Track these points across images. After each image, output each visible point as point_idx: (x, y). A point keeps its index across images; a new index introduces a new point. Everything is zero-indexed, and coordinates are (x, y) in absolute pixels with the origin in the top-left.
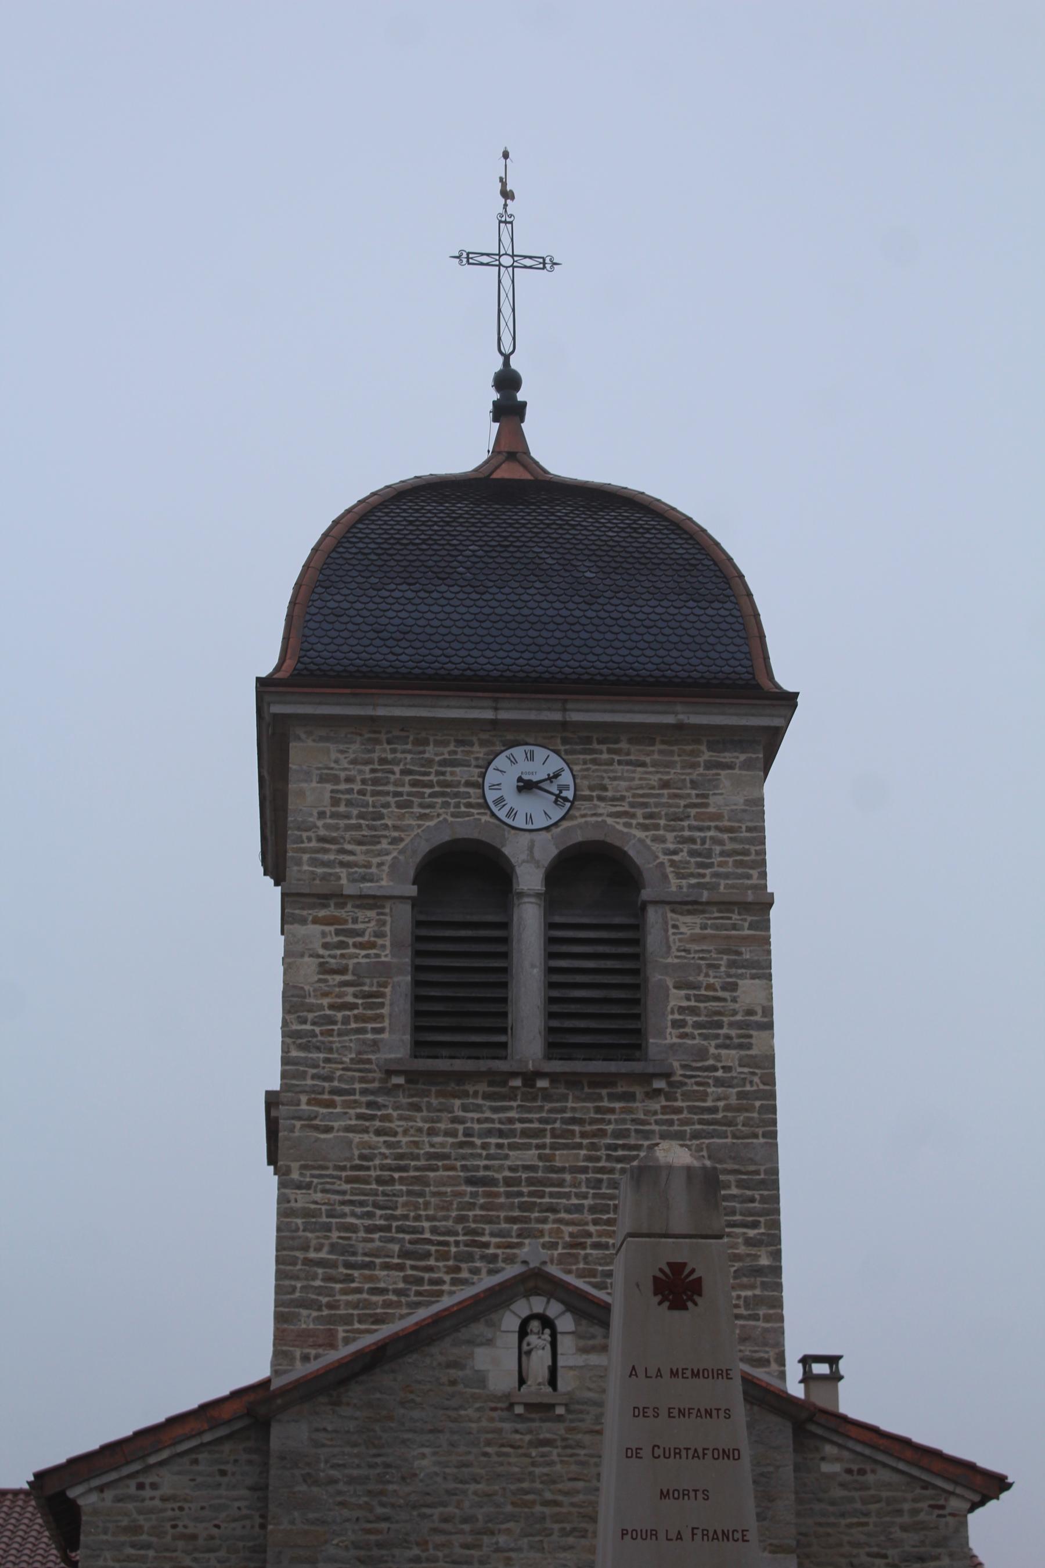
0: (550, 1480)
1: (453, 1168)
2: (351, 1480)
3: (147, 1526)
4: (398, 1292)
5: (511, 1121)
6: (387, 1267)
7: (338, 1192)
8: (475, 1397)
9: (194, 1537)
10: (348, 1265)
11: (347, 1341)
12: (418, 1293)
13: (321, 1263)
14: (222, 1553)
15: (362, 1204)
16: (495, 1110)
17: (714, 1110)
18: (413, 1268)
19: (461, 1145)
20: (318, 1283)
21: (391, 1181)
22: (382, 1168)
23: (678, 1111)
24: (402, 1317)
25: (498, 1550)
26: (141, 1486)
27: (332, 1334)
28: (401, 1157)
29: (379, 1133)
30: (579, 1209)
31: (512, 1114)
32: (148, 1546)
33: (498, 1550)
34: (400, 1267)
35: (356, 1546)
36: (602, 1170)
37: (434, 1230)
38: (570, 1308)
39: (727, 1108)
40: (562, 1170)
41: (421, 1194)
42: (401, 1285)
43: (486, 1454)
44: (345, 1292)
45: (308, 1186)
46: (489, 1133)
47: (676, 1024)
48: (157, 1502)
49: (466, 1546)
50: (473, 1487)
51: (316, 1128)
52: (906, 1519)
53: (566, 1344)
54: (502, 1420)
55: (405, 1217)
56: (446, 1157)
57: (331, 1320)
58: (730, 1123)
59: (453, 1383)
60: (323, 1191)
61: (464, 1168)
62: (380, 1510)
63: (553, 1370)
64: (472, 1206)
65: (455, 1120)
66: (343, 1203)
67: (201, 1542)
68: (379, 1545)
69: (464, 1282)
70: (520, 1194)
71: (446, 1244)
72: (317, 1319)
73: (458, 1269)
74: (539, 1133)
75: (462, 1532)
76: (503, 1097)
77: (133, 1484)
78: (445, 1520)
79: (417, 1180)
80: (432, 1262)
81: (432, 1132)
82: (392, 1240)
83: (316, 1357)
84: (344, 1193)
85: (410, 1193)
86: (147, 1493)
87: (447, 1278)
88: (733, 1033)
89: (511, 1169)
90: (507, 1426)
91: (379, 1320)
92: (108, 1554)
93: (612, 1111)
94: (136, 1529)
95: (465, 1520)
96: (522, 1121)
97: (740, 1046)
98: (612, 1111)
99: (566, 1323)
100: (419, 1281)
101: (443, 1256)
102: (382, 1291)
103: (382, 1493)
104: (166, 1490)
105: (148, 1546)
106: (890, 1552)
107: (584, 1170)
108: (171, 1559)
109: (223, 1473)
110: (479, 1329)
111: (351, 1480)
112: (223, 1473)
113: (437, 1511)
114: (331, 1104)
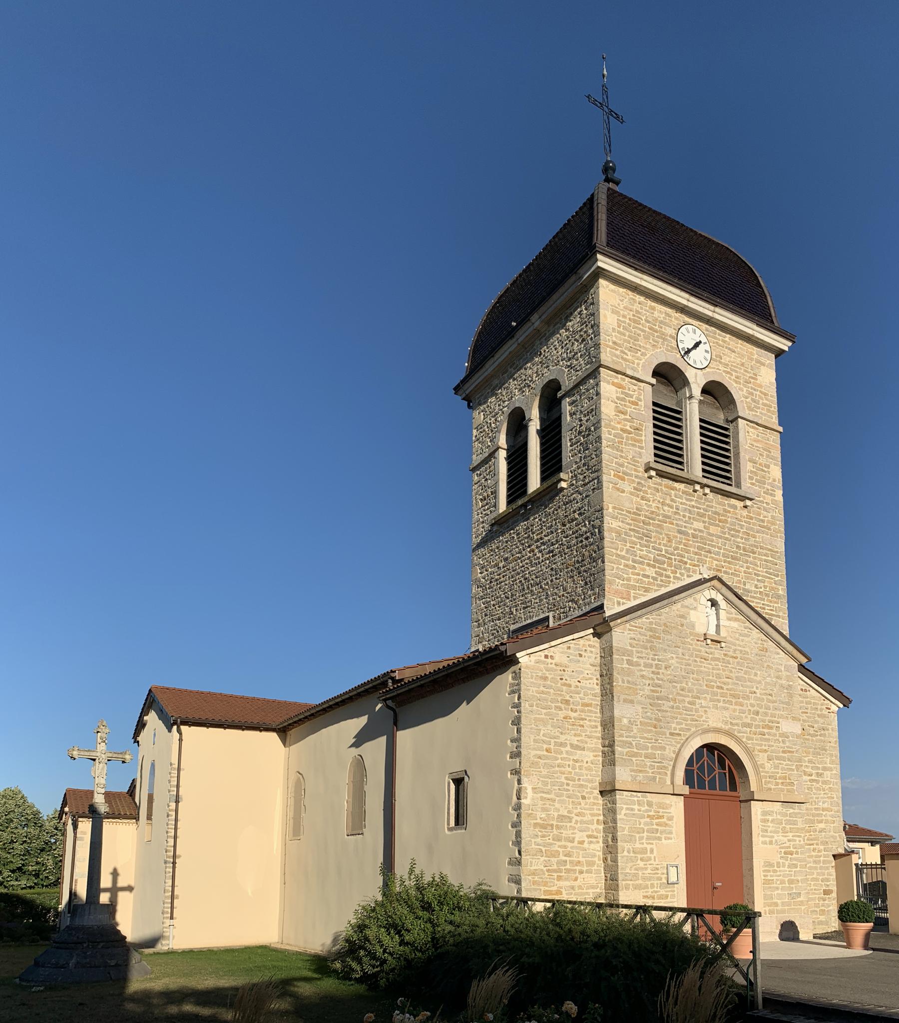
0: (718, 676)
1: (673, 524)
2: (646, 665)
3: (550, 677)
4: (655, 579)
5: (693, 506)
6: (649, 565)
7: (628, 524)
8: (691, 634)
9: (570, 686)
10: (634, 561)
11: (635, 598)
12: (662, 581)
13: (623, 557)
14: (581, 695)
15: (637, 532)
16: (687, 500)
17: (763, 521)
18: (659, 568)
19: (676, 513)
20: (622, 567)
21: (649, 524)
22: (646, 516)
23: (751, 518)
24: (656, 590)
25: (702, 707)
26: (546, 657)
27: (629, 594)
28: (652, 513)
29: (643, 498)
30: (718, 554)
31: (693, 503)
32: (551, 687)
33: (702, 707)
34: (654, 567)
35: (648, 697)
36: (726, 539)
37: (666, 552)
38: (726, 599)
39: (768, 522)
40: (712, 535)
41: (661, 534)
42: (654, 575)
43: (696, 661)
44: (633, 574)
45: (617, 518)
46: (686, 509)
47: (751, 478)
48: (553, 666)
49: (689, 703)
50: (691, 676)
51: (618, 489)
52: (819, 712)
53: (722, 614)
54: (701, 646)
55: (655, 542)
56: (669, 517)
57: (628, 587)
58: (769, 529)
59: (682, 625)
60: (622, 522)
61: (677, 525)
62: (656, 681)
63: (718, 626)
64: (680, 543)
65: (672, 500)
66: (630, 530)
67: (573, 688)
68: (658, 698)
69: (678, 578)
70: (697, 542)
71: (671, 559)
72: (622, 585)
73: (676, 572)
74: (703, 515)
75: (688, 696)
76: (690, 495)
77: (542, 654)
78: (682, 690)
79: (659, 526)
80: (665, 566)
81: (663, 504)
82: (650, 552)
83: (623, 604)
84: (630, 525)
85: (657, 532)
86: (549, 660)
87: (672, 575)
88: (769, 488)
89: (695, 530)
90: (703, 649)
91: (647, 590)
92: (535, 689)
93: (729, 512)
94: (545, 678)
95: (689, 692)
96: (698, 508)
97: (771, 495)
98: (729, 512)
99: (722, 604)
100: (661, 575)
101: (670, 565)
102: (648, 577)
103: (658, 673)
104: (557, 659)
105: (551, 687)
106: (816, 726)
107: (720, 537)
108: (561, 695)
109: (581, 655)
110: (689, 601)
111: (646, 665)
112: (581, 655)
113: (679, 685)
114: (623, 479)
